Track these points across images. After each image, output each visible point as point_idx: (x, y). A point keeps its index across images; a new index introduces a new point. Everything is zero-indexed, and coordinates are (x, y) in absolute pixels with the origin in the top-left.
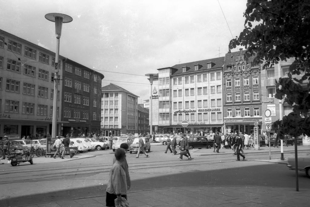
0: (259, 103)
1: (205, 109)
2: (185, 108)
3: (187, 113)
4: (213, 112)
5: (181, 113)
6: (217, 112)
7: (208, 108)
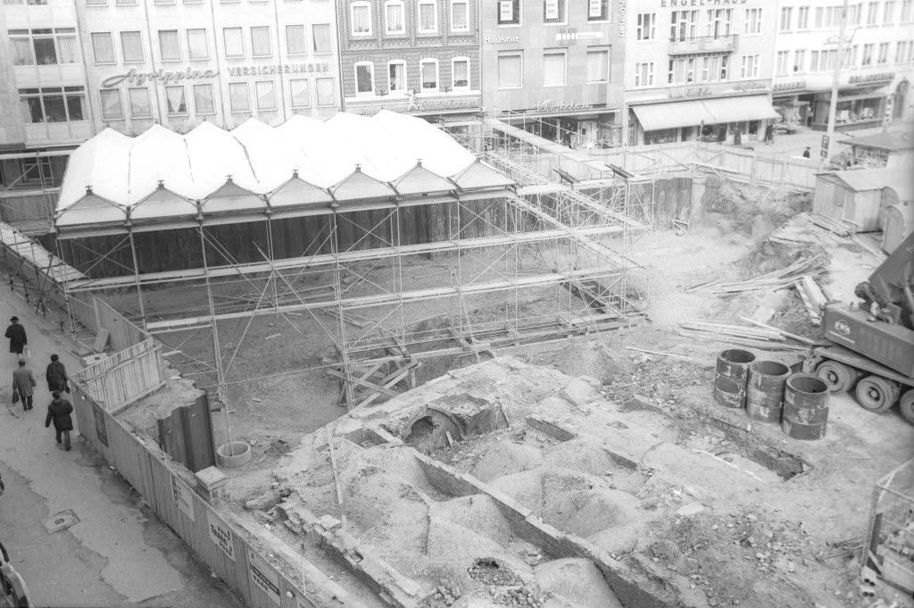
0: (470, 43)
1: (260, 65)
2: (157, 58)
3: (171, 83)
4: (300, 76)
5: (140, 82)
6: (316, 75)
7: (275, 62)
